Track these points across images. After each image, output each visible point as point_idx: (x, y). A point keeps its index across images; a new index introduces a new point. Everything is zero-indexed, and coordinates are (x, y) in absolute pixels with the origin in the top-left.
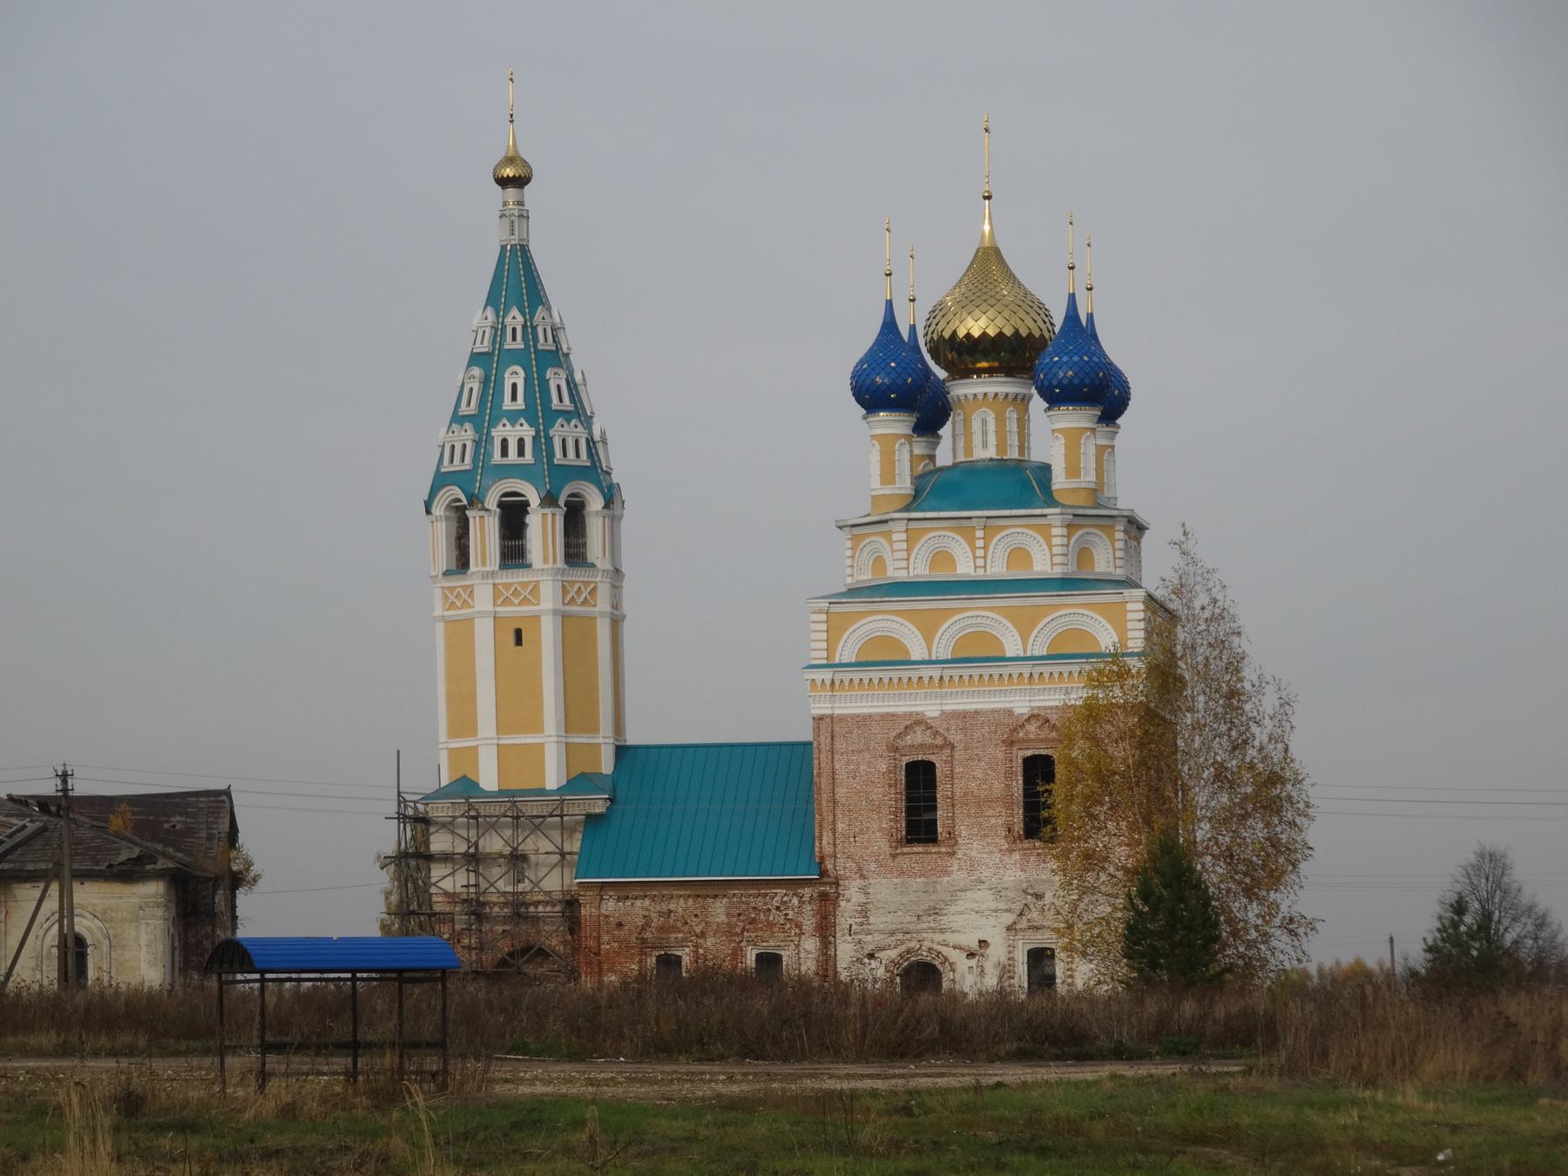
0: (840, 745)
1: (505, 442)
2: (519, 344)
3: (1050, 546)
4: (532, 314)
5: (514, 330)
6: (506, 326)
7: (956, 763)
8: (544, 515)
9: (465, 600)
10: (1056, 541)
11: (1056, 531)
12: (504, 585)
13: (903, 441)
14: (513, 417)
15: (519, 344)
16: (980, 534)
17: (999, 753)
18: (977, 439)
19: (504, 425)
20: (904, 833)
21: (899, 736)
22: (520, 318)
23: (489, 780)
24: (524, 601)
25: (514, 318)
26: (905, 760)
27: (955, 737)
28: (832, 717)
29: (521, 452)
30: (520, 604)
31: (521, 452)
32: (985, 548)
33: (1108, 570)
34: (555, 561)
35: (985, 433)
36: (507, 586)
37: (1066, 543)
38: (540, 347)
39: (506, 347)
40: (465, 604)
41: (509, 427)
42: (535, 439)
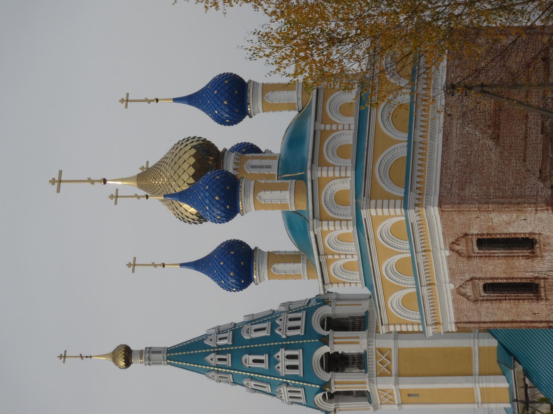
0: (475, 319)
1: (288, 367)
2: (228, 357)
3: (334, 178)
4: (210, 347)
5: (220, 360)
6: (217, 365)
7: (484, 276)
8: (334, 343)
10: (331, 174)
11: (324, 174)
13: (272, 270)
14: (273, 362)
15: (228, 357)
16: (330, 257)
17: (475, 262)
18: (265, 171)
19: (279, 367)
20: (532, 295)
21: (468, 298)
22: (212, 355)
25: (212, 359)
26: (483, 294)
27: (468, 277)
28: (456, 323)
29: (295, 357)
30: (390, 360)
31: (295, 357)
32: (339, 255)
33: (349, 182)
34: (364, 383)
35: (261, 167)
37: (332, 168)
38: (230, 343)
39: (230, 365)
40: (390, 394)
41: (279, 365)
42: (287, 348)
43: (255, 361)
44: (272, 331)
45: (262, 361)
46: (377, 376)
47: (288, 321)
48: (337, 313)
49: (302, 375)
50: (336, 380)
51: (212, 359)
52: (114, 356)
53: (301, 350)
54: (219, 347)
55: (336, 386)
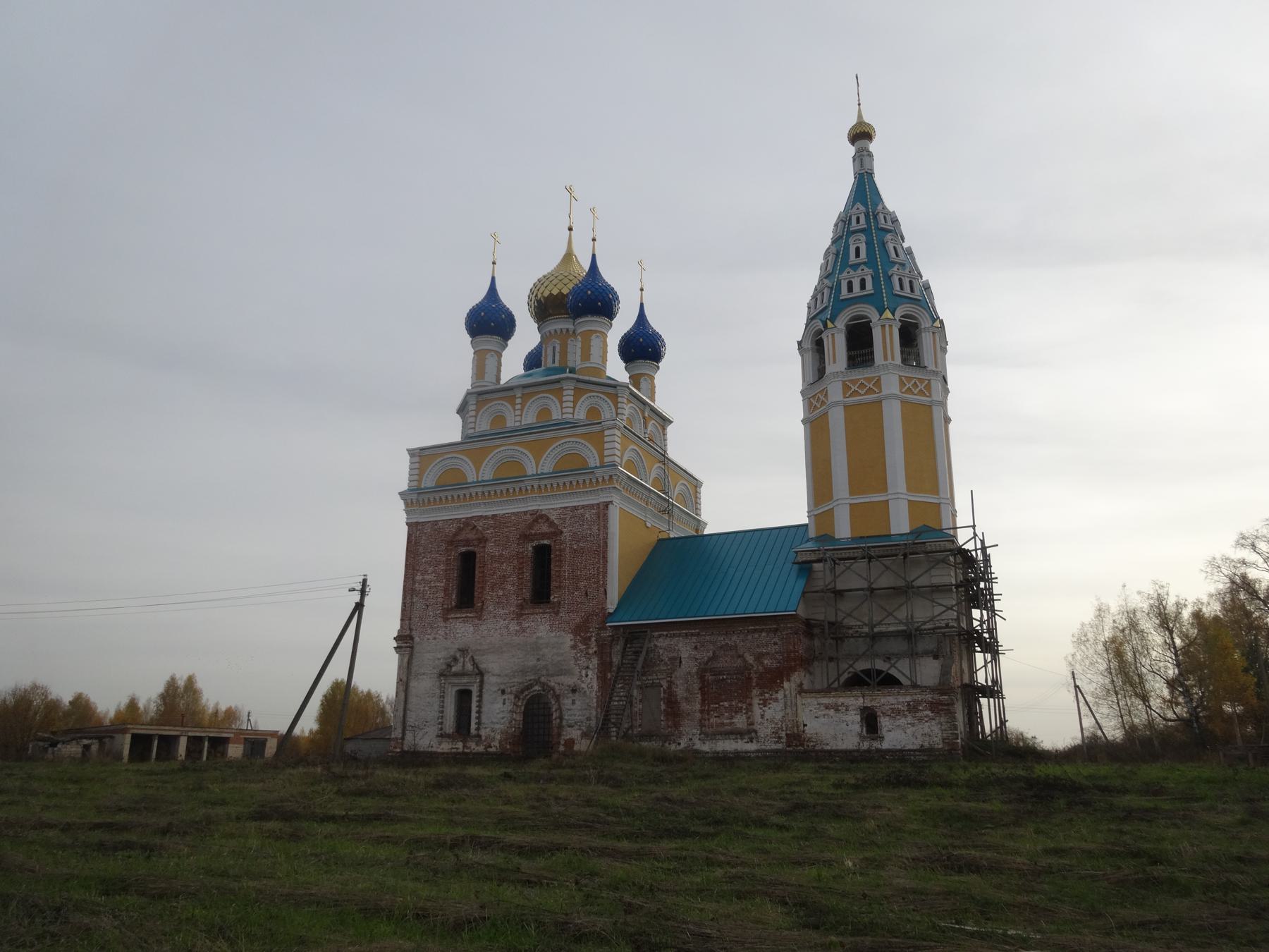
9: (823, 401)
12: (851, 381)
14: (855, 267)
23: (843, 530)
24: (870, 391)
29: (863, 286)
30: (865, 394)
31: (863, 286)
36: (854, 382)
40: (823, 403)
41: (852, 273)
43: (858, 250)
44: (894, 263)
45: (858, 255)
46: (844, 382)
47: (909, 279)
48: (923, 334)
49: (841, 298)
50: (835, 335)
51: (858, 209)
52: (861, 123)
53: (872, 292)
54: (875, 217)
55: (830, 337)
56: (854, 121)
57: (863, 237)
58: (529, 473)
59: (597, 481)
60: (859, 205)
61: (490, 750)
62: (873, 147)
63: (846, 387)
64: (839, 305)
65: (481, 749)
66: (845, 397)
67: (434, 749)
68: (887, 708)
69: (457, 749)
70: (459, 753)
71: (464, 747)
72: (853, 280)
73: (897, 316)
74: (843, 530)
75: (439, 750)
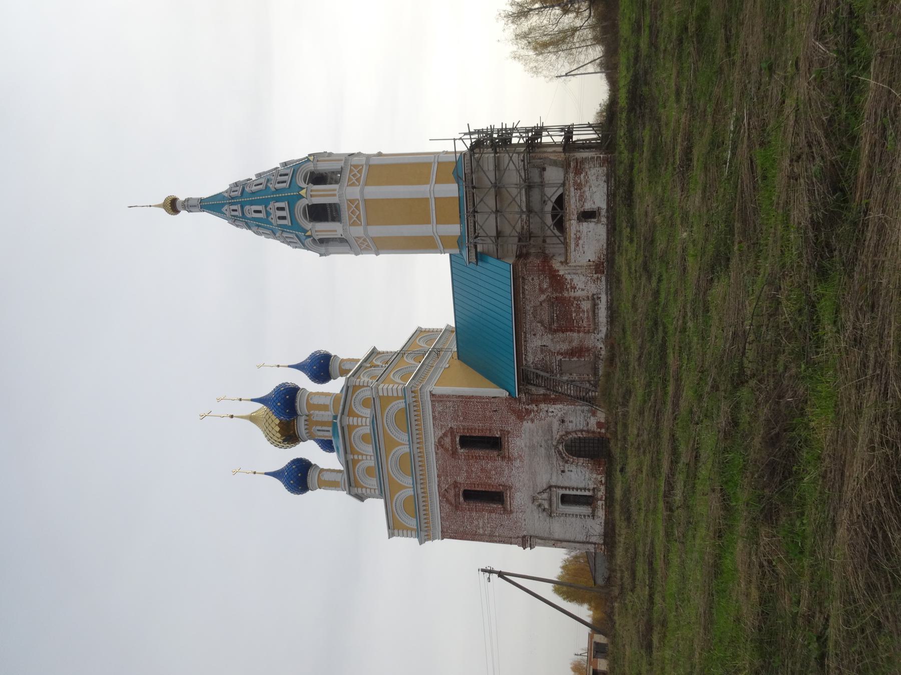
9: (363, 240)
12: (350, 220)
24: (357, 207)
29: (282, 209)
30: (359, 211)
31: (282, 209)
36: (350, 218)
41: (272, 216)
43: (256, 212)
44: (266, 185)
45: (259, 212)
46: (350, 225)
48: (318, 168)
49: (290, 224)
52: (164, 206)
53: (286, 202)
54: (232, 198)
56: (163, 210)
57: (247, 208)
58: (412, 493)
59: (420, 452)
60: (224, 209)
61: (603, 482)
62: (182, 197)
63: (354, 224)
64: (295, 226)
65: (603, 488)
66: (361, 225)
67: (603, 521)
68: (578, 204)
69: (602, 505)
70: (606, 503)
71: (601, 500)
72: (277, 216)
73: (303, 185)
74: (454, 229)
75: (604, 517)
